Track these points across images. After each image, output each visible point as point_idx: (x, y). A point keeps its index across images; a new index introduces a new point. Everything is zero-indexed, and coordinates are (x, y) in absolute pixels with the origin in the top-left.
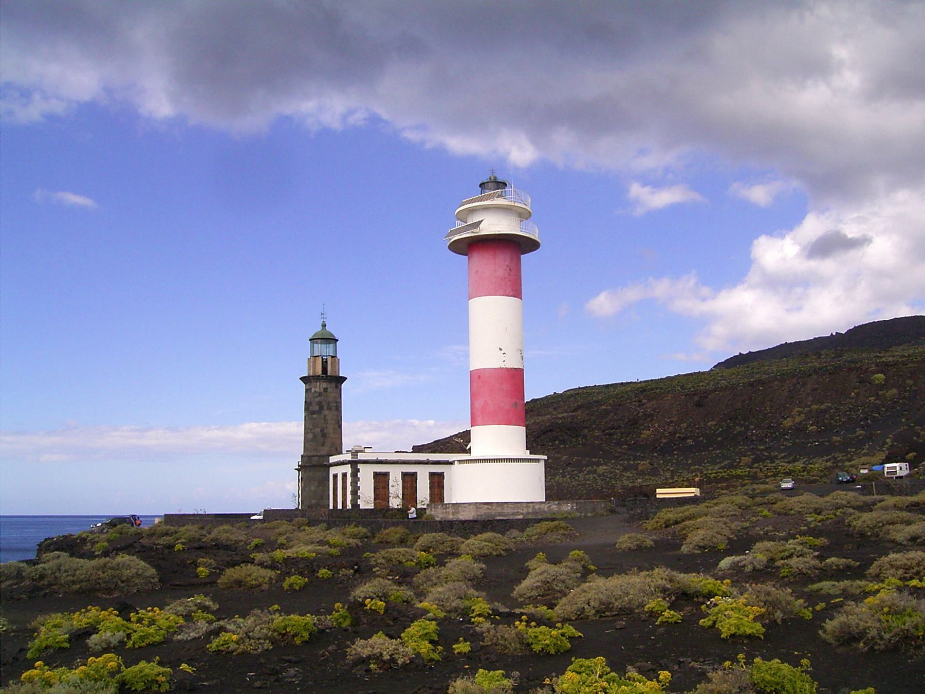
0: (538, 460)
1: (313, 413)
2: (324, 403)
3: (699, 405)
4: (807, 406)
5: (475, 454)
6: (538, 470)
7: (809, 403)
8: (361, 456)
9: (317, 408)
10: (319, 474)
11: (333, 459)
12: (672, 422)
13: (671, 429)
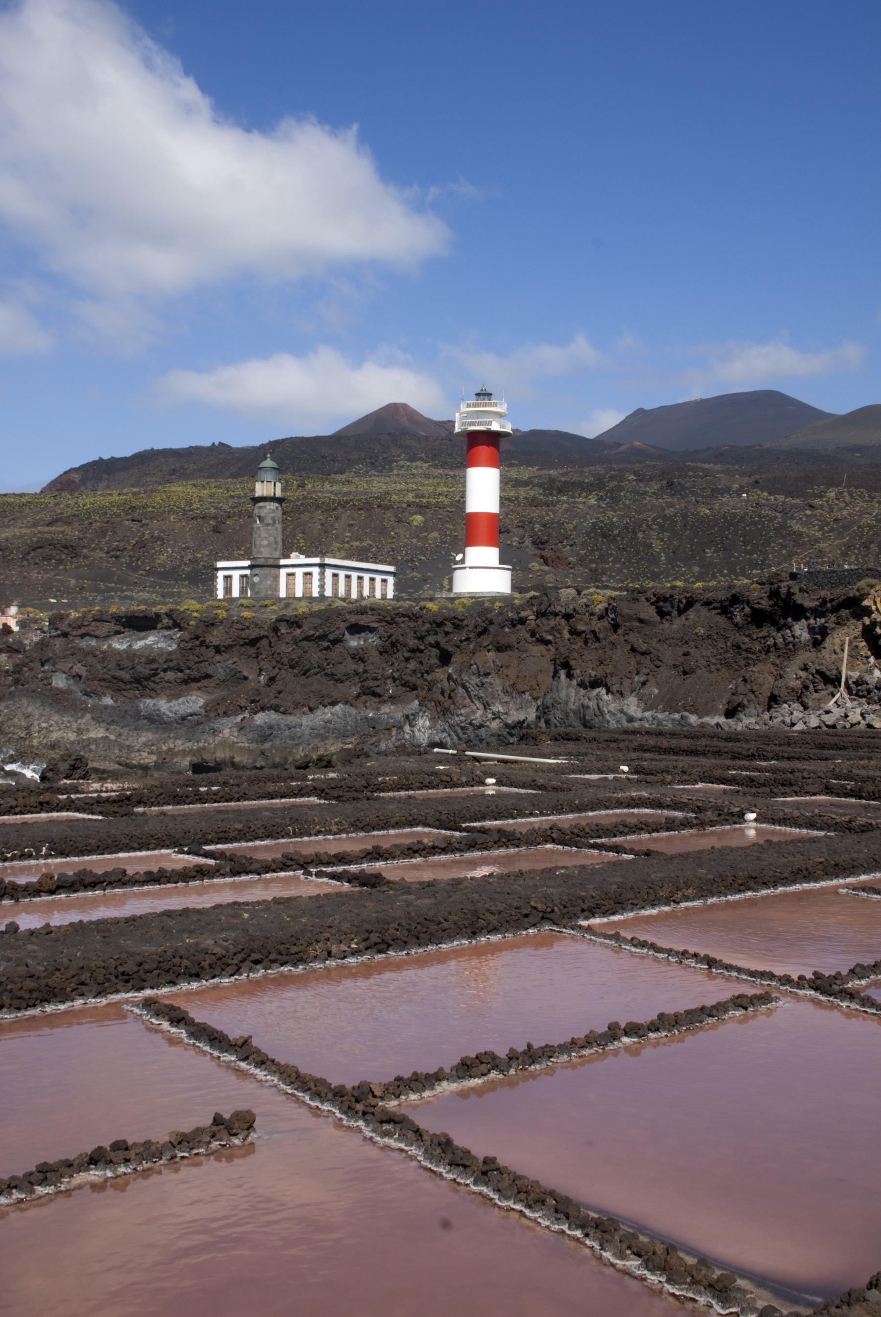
0: (509, 569)
1: (268, 525)
2: (276, 519)
3: (216, 530)
4: (344, 542)
5: (468, 563)
6: (508, 574)
7: (347, 539)
8: (328, 561)
9: (271, 522)
10: (274, 571)
11: (283, 562)
12: (188, 548)
13: (190, 556)
